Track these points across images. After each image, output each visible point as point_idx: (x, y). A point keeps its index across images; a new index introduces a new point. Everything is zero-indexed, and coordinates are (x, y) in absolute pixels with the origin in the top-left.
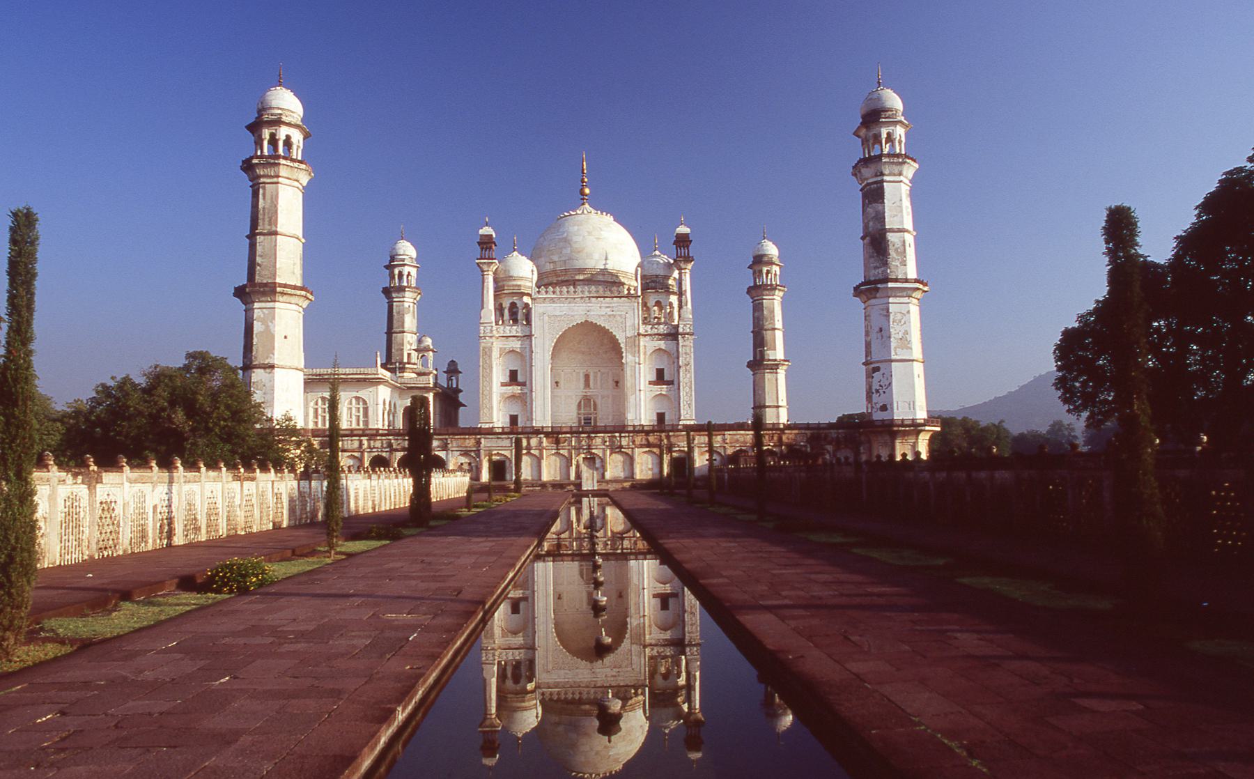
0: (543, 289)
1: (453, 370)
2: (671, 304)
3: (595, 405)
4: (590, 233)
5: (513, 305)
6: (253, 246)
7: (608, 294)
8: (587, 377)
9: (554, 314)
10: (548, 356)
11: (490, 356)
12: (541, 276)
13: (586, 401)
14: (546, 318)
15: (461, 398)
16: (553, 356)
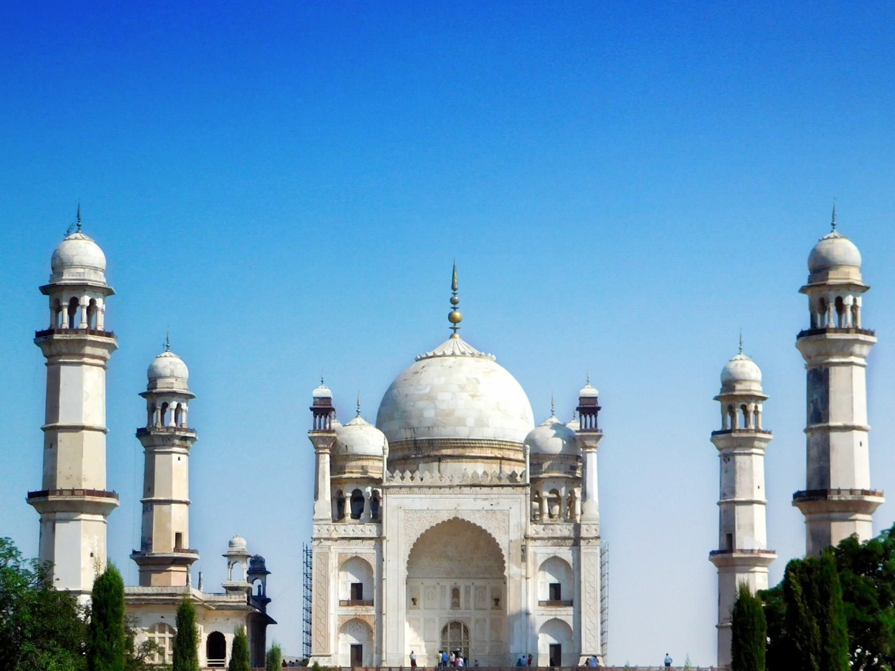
0: (398, 474)
1: (258, 569)
2: (572, 493)
3: (466, 631)
4: (462, 388)
5: (357, 498)
6: (51, 444)
7: (487, 483)
8: (456, 592)
9: (411, 511)
10: (403, 566)
11: (326, 565)
12: (393, 444)
13: (455, 629)
14: (402, 514)
15: (271, 610)
16: (408, 562)
